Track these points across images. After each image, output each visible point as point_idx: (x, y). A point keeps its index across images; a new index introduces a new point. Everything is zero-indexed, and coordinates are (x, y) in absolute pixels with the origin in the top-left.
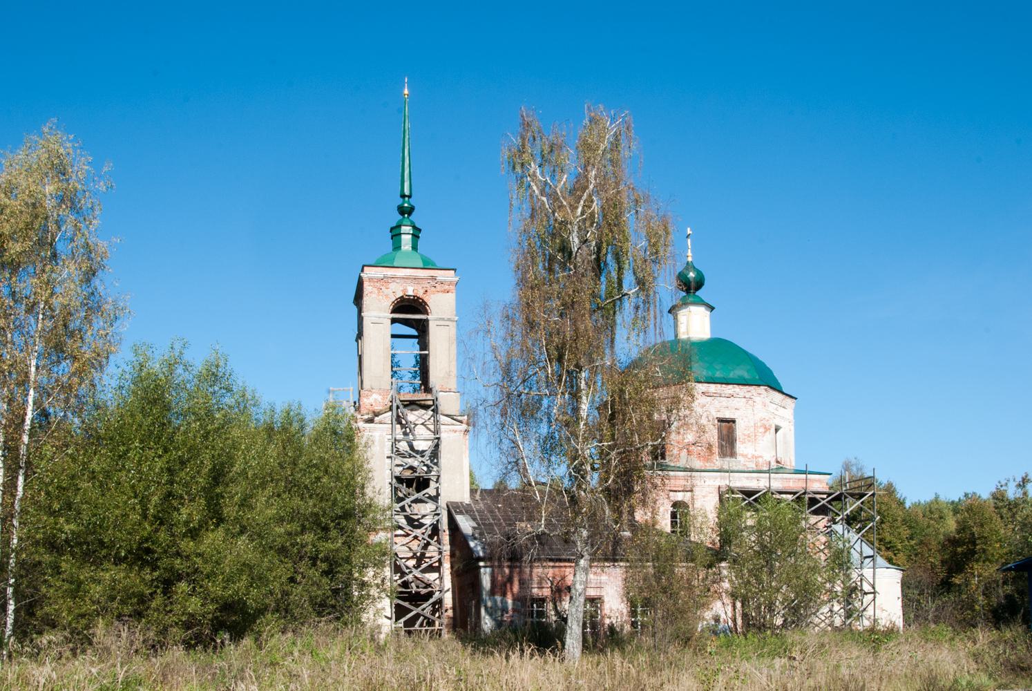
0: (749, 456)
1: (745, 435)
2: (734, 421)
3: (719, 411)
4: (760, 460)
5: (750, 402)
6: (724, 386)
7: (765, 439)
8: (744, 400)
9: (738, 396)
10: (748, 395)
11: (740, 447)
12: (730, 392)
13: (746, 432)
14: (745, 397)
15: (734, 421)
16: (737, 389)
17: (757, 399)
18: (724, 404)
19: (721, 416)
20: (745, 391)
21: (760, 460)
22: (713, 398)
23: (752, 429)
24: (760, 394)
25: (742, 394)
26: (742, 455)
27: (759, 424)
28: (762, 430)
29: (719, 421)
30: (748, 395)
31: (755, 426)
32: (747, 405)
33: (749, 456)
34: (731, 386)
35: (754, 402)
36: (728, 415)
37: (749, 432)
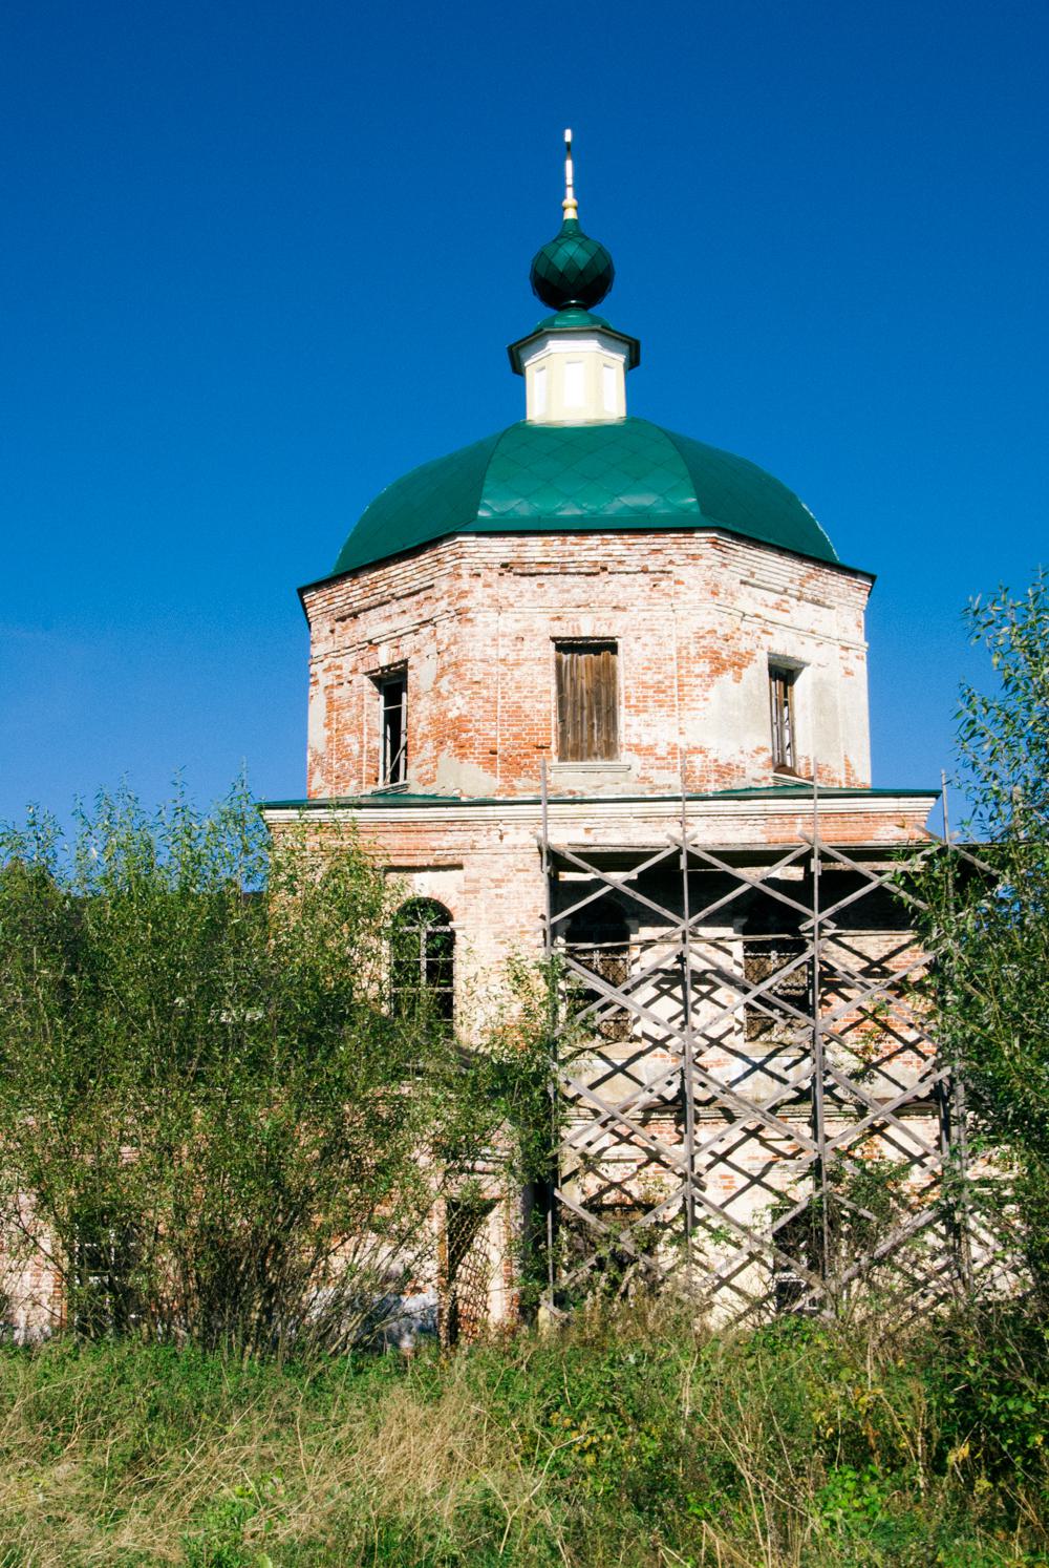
0: (661, 751)
1: (644, 685)
2: (610, 646)
3: (559, 618)
4: (697, 759)
5: (663, 584)
6: (571, 539)
7: (713, 693)
8: (646, 578)
9: (621, 568)
10: (653, 563)
11: (630, 726)
12: (594, 556)
13: (650, 678)
14: (645, 571)
15: (610, 646)
16: (617, 545)
17: (686, 573)
18: (578, 595)
19: (565, 631)
20: (645, 549)
21: (697, 759)
22: (540, 580)
23: (671, 667)
24: (695, 557)
25: (633, 563)
26: (637, 749)
27: (693, 651)
28: (704, 667)
29: (559, 648)
30: (653, 563)
31: (682, 657)
32: (655, 595)
33: (661, 751)
34: (594, 540)
35: (678, 582)
36: (587, 627)
37: (660, 677)
